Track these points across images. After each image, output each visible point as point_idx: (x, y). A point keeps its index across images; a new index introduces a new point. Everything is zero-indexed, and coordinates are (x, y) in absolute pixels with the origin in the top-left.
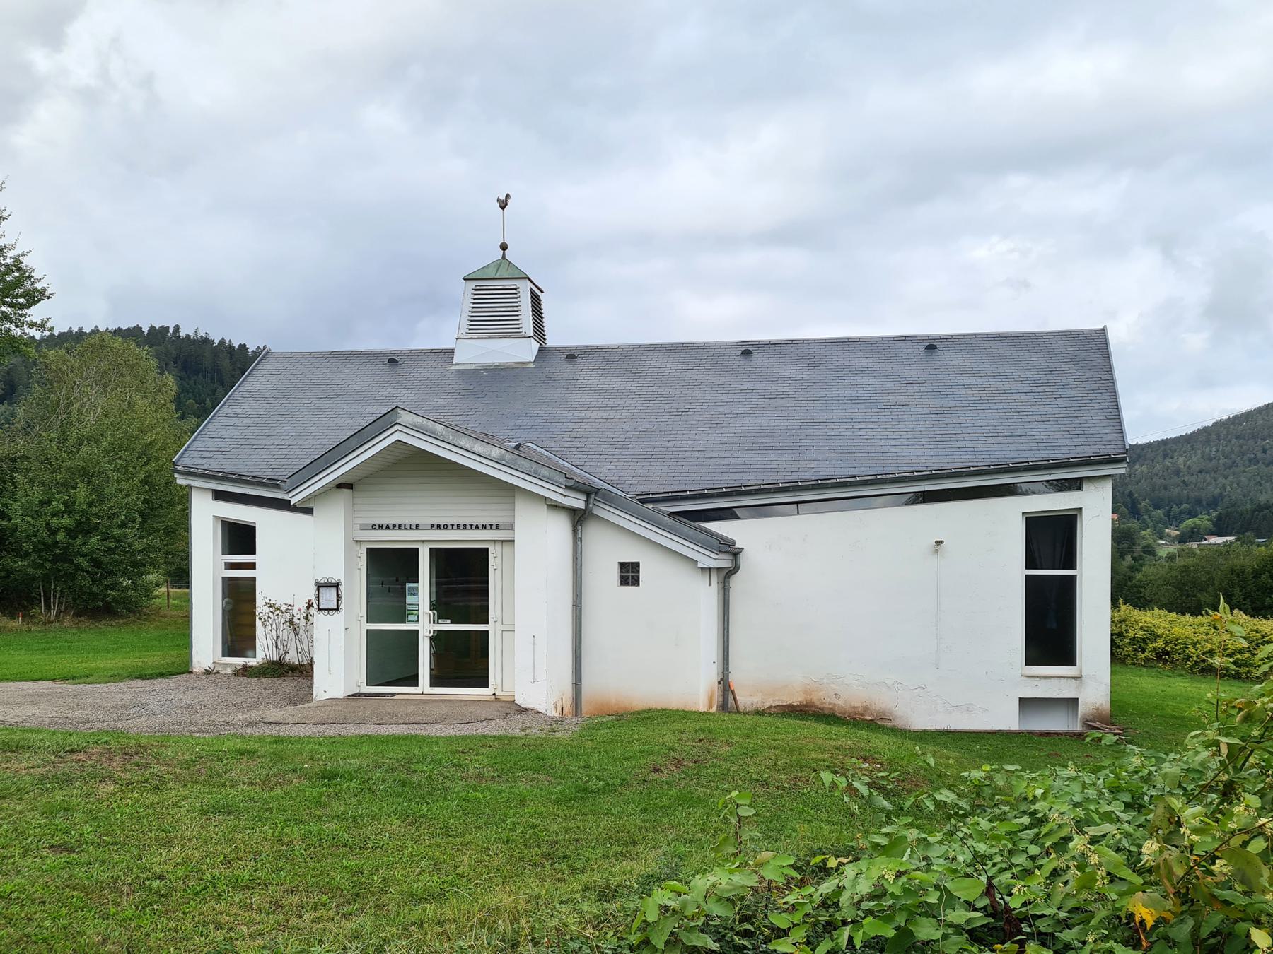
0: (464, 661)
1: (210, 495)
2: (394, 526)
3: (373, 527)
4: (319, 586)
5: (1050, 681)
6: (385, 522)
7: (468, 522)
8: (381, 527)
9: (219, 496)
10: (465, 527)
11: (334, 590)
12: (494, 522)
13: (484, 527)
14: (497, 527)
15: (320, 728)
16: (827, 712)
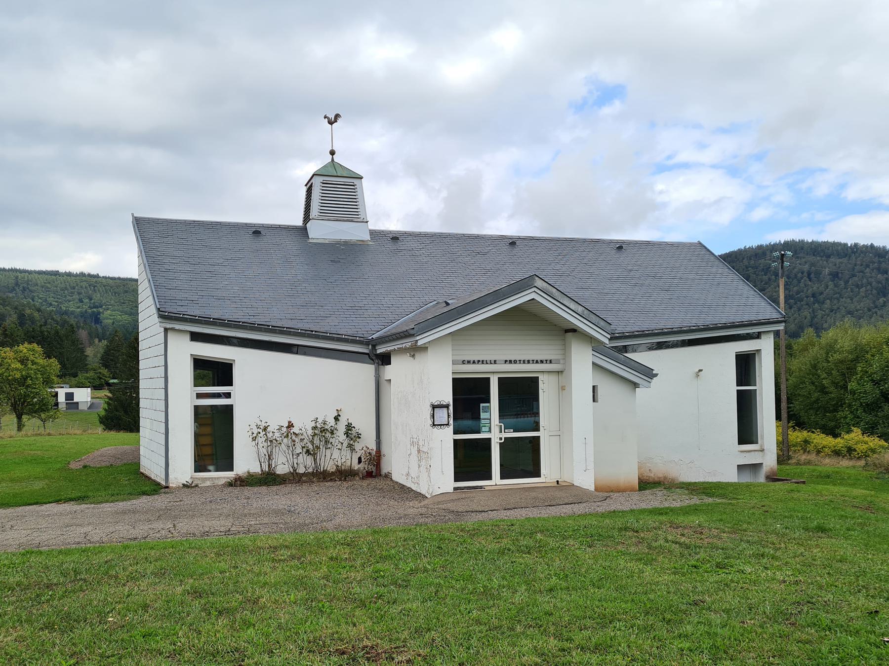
0: (523, 458)
1: (188, 337)
2: (479, 361)
3: (463, 362)
4: (434, 407)
5: (748, 455)
6: (472, 359)
7: (531, 358)
8: (469, 362)
9: (196, 337)
10: (529, 362)
11: (445, 410)
12: (549, 358)
13: (542, 362)
14: (551, 362)
15: (508, 513)
16: (651, 480)
